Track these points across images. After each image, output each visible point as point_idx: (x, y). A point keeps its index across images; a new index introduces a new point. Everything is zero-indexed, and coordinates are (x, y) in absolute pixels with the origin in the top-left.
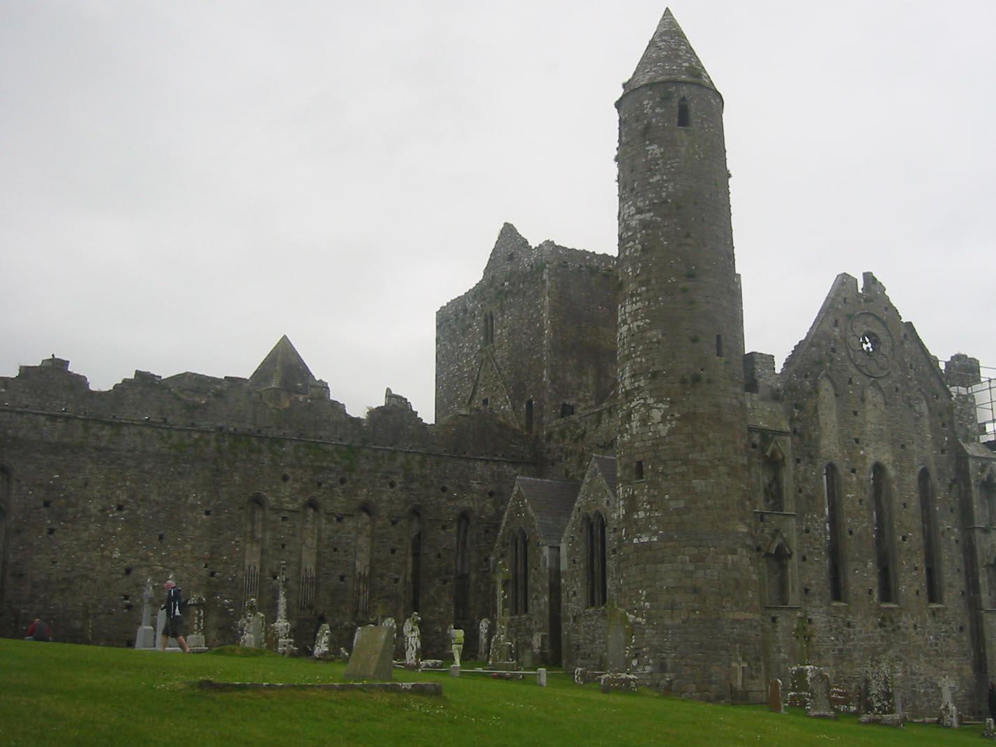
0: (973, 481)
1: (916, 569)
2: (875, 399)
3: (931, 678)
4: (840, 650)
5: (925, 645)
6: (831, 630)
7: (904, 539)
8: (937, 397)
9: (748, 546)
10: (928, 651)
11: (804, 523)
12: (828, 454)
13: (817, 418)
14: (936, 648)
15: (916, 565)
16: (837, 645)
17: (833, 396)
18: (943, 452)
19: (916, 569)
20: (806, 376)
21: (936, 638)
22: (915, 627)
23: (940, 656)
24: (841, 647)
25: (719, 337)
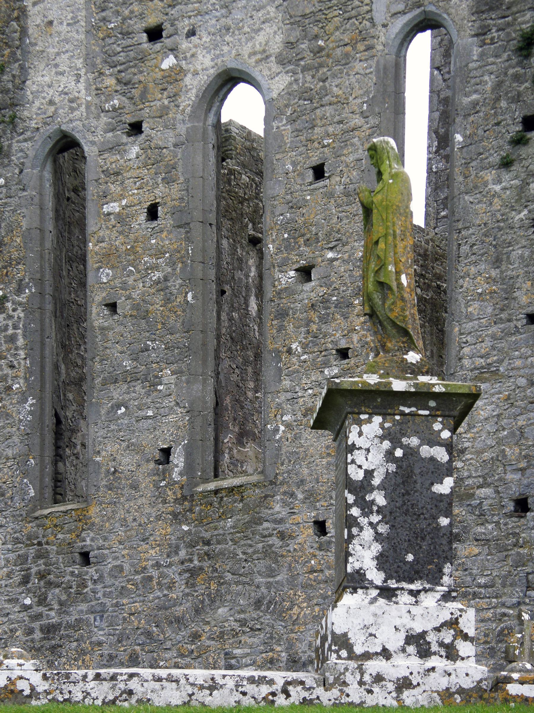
15: (343, 344)
19: (343, 354)
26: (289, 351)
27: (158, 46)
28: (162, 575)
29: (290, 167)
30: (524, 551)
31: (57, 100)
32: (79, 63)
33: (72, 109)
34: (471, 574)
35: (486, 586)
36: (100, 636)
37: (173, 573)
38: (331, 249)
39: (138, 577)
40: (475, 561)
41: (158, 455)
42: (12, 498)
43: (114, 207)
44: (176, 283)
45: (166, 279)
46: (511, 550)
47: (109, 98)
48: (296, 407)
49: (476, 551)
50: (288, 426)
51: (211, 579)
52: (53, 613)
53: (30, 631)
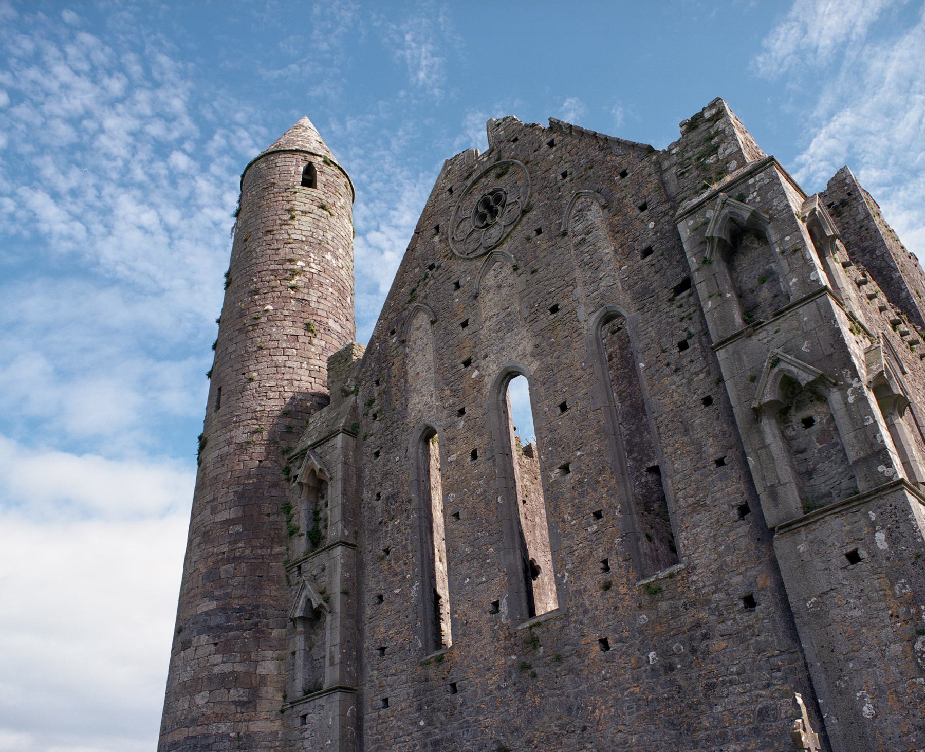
1: (598, 515)
2: (500, 276)
6: (420, 709)
7: (565, 469)
9: (208, 629)
16: (428, 735)
19: (598, 515)
22: (604, 643)
26: (564, 521)
27: (470, 368)
32: (432, 388)
33: (430, 411)
34: (723, 665)
35: (739, 674)
37: (509, 693)
38: (579, 449)
39: (487, 698)
40: (725, 653)
41: (490, 607)
46: (750, 639)
47: (448, 400)
48: (574, 557)
49: (724, 644)
51: (535, 694)
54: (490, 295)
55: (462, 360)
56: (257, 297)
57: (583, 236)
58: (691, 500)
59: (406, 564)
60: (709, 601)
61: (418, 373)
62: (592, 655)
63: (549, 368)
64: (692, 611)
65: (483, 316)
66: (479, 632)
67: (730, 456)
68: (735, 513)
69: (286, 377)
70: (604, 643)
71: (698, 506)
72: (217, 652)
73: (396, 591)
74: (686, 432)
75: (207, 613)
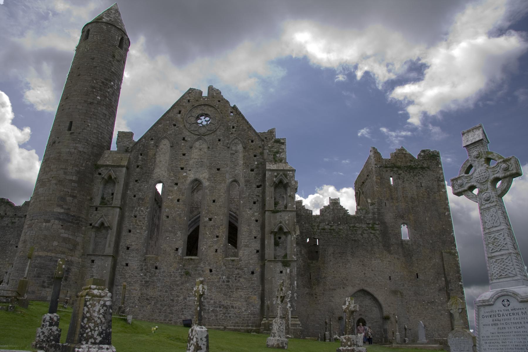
0: (267, 184)
1: (217, 237)
2: (201, 146)
3: (220, 302)
4: (146, 282)
5: (218, 282)
6: (142, 270)
7: (210, 219)
8: (252, 141)
9: (60, 219)
10: (222, 285)
11: (134, 212)
12: (159, 176)
13: (156, 158)
14: (228, 283)
15: (218, 235)
16: (144, 278)
17: (169, 147)
18: (252, 170)
19: (217, 237)
20: (152, 139)
21: (228, 278)
22: (211, 271)
23: (230, 288)
24: (148, 280)
25: (71, 123)
26: (206, 234)
28: (174, 275)
29: (208, 199)
30: (253, 282)
31: (161, 175)
32: (166, 169)
33: (164, 177)
35: (245, 288)
36: (158, 285)
37: (177, 274)
39: (169, 274)
41: (175, 249)
42: (140, 252)
43: (170, 197)
44: (182, 215)
45: (180, 214)
47: (172, 177)
49: (244, 280)
50: (205, 249)
52: (148, 278)
53: (142, 281)
54: (197, 151)
55: (180, 166)
56: (94, 90)
57: (234, 152)
58: (245, 244)
59: (143, 224)
60: (243, 269)
61: (161, 161)
62: (206, 272)
63: (212, 187)
64: (238, 270)
65: (192, 156)
66: (170, 254)
67: (259, 236)
68: (256, 251)
69: (100, 131)
70: (211, 271)
71: (246, 246)
72: (62, 229)
73: (138, 231)
74: (249, 226)
75: (59, 213)
